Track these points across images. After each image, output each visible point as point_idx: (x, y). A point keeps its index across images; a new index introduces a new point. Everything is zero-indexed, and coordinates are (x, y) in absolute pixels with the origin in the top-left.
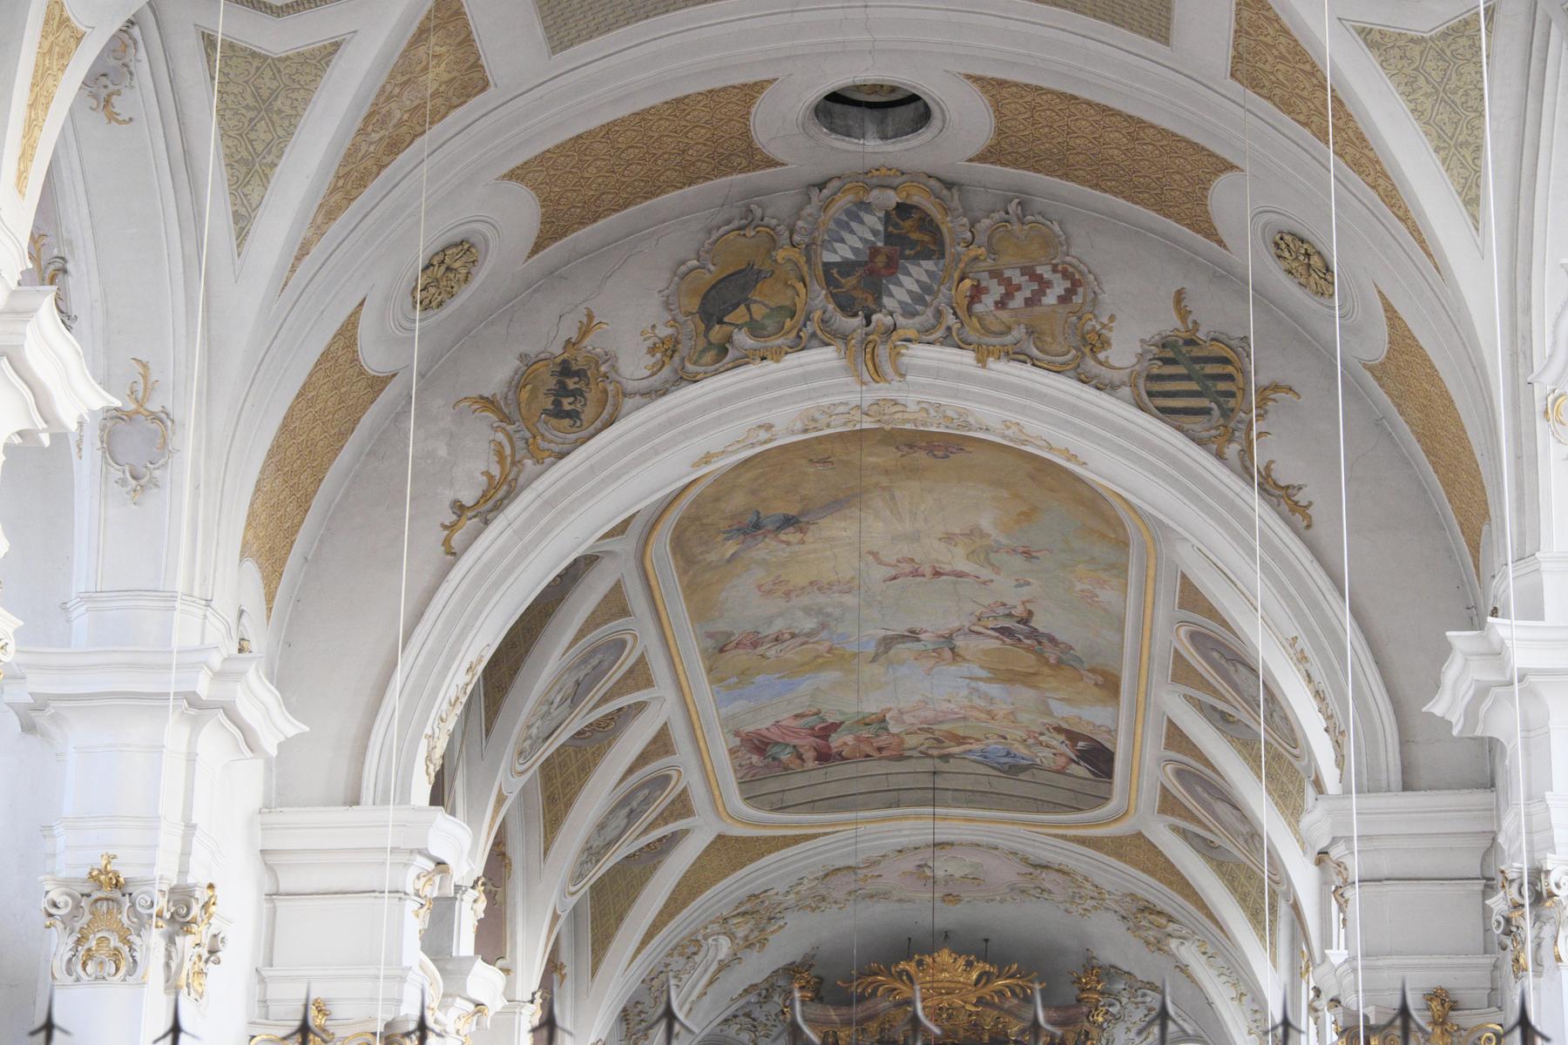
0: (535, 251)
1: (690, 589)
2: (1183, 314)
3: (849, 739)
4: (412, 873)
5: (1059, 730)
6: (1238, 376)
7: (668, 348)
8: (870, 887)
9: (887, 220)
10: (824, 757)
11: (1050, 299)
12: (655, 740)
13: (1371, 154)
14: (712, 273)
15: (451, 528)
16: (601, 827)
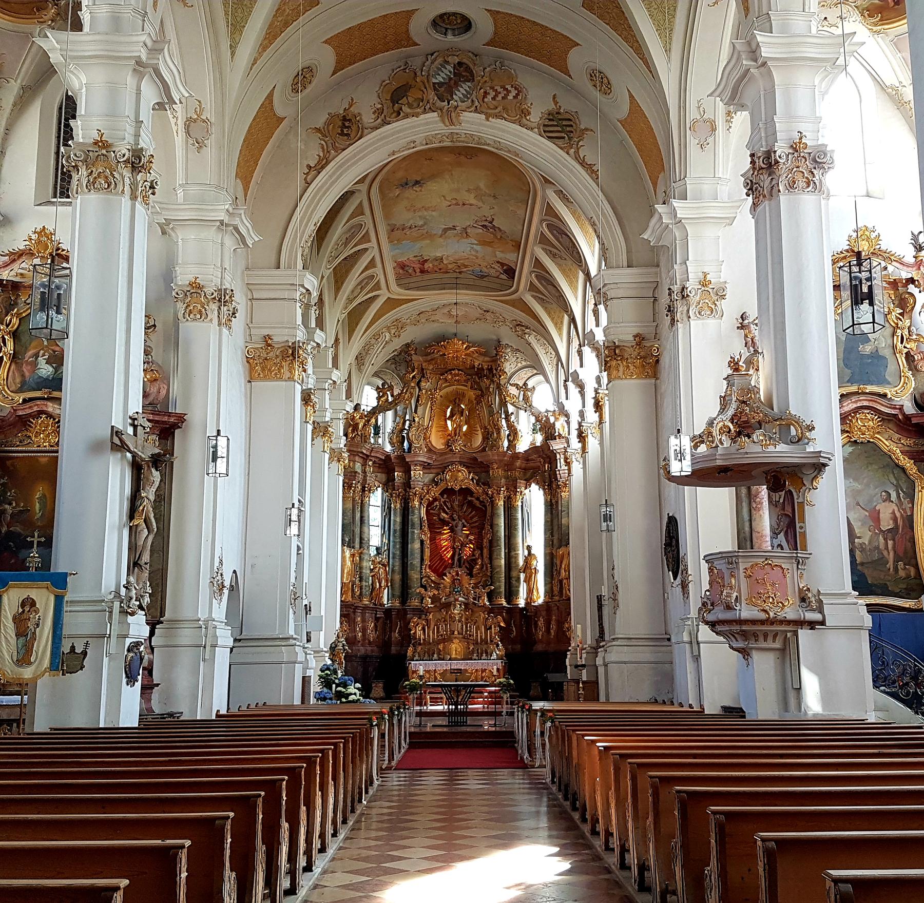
0: (332, 75)
1: (384, 207)
2: (556, 103)
3: (431, 265)
4: (298, 293)
5: (498, 262)
6: (574, 125)
7: (379, 112)
8: (433, 318)
9: (454, 68)
10: (422, 271)
11: (510, 97)
12: (370, 262)
13: (632, 33)
14: (395, 85)
15: (307, 174)
16: (353, 291)
